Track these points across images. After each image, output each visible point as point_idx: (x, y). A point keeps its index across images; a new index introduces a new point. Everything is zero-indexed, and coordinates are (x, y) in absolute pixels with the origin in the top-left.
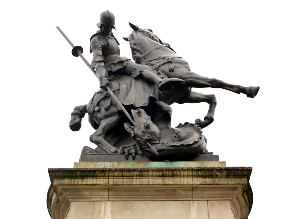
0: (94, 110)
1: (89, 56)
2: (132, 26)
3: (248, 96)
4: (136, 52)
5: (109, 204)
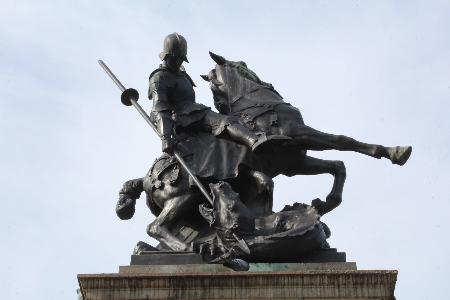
0: (155, 186)
1: (148, 104)
2: (214, 56)
4: (219, 97)
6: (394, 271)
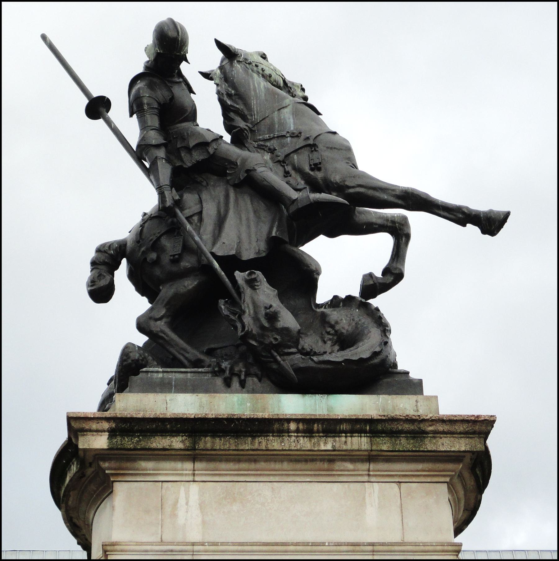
0: (146, 259)
1: (132, 130)
2: (219, 44)
3: (484, 231)
4: (232, 115)
5: (194, 488)
6: (491, 416)
